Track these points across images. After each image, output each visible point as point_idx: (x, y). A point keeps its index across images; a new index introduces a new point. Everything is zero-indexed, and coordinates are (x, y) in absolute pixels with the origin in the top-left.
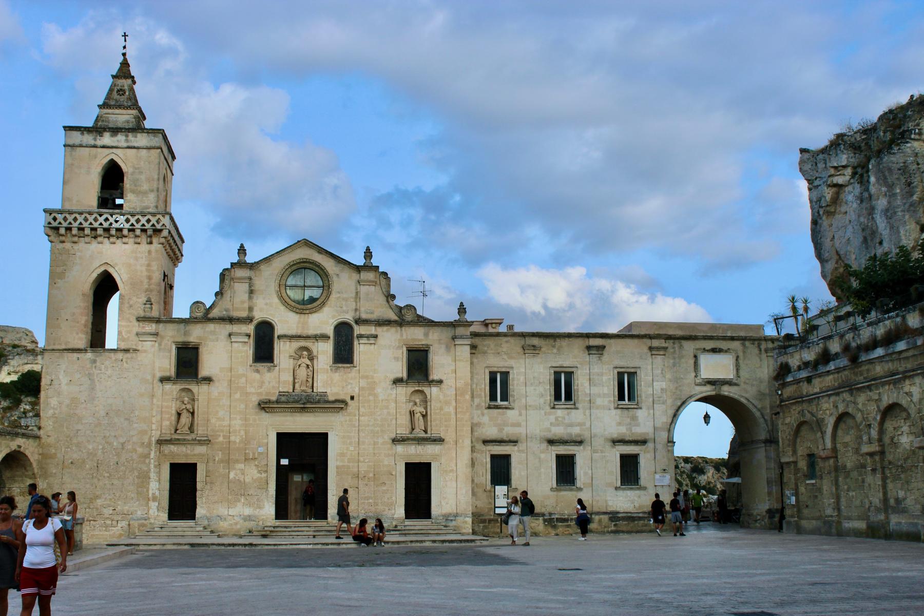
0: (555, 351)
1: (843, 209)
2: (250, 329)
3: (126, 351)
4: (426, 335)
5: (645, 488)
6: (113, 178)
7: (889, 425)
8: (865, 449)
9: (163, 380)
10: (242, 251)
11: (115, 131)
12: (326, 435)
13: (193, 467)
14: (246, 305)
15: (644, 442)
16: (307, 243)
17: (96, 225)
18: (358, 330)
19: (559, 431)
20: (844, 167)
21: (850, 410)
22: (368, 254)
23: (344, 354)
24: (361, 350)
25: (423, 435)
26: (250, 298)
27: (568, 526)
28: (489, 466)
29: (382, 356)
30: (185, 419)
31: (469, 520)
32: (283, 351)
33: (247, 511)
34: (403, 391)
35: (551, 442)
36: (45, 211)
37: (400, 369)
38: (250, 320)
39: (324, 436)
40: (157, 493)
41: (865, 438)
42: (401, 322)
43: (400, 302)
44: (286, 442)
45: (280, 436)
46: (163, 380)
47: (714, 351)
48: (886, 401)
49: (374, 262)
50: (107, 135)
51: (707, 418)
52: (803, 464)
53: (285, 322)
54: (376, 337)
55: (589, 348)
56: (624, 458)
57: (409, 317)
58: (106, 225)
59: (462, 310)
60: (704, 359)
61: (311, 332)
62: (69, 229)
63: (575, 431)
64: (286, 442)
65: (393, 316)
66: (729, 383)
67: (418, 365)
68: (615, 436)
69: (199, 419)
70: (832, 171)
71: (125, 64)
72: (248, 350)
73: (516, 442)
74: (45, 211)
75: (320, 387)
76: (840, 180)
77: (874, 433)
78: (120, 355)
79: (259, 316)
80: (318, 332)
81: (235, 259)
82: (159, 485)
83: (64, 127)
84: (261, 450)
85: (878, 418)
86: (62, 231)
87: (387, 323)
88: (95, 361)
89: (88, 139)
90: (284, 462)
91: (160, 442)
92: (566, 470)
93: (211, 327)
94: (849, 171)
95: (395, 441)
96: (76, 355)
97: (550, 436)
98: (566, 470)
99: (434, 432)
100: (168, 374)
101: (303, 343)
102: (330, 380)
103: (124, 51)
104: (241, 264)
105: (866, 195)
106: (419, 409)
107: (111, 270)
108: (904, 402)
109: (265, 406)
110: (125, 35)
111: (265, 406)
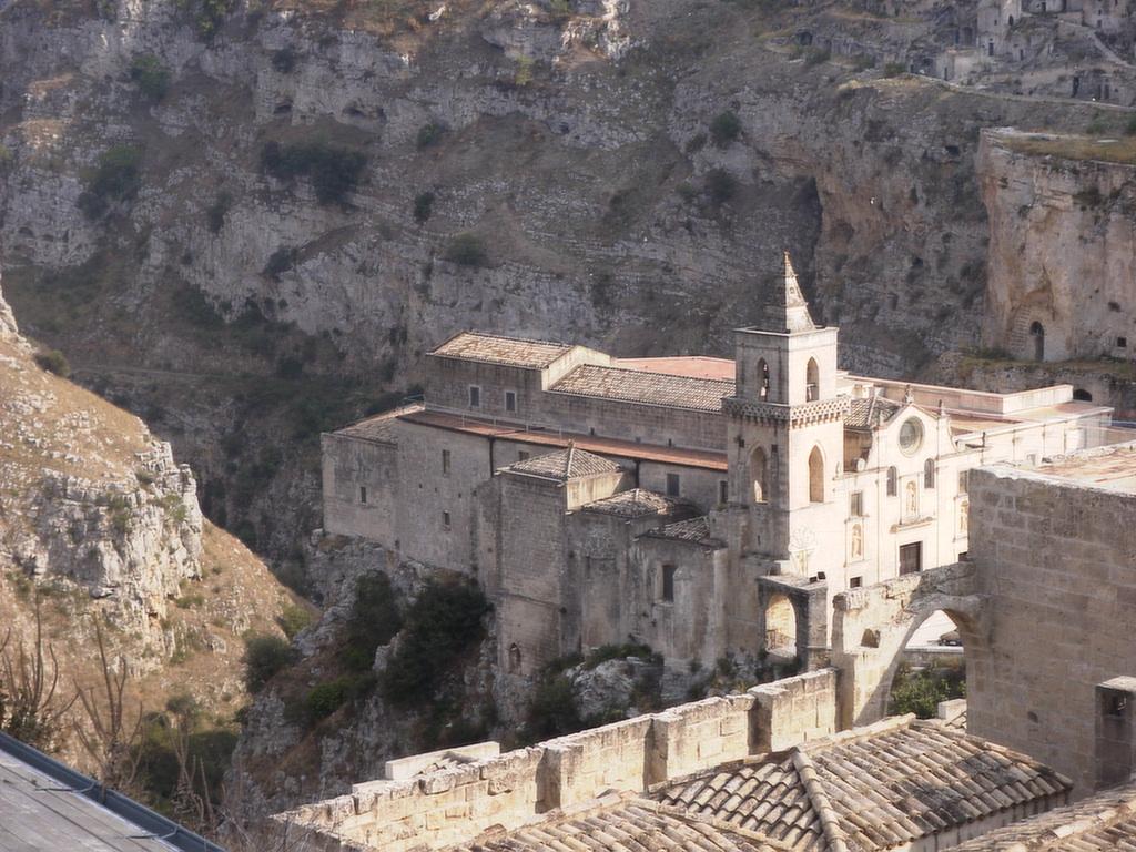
1: (1055, 229)
2: (883, 477)
20: (1064, 193)
29: (948, 480)
32: (901, 485)
39: (918, 546)
42: (957, 454)
70: (1050, 194)
72: (884, 487)
76: (1058, 204)
107: (819, 446)
109: (893, 529)
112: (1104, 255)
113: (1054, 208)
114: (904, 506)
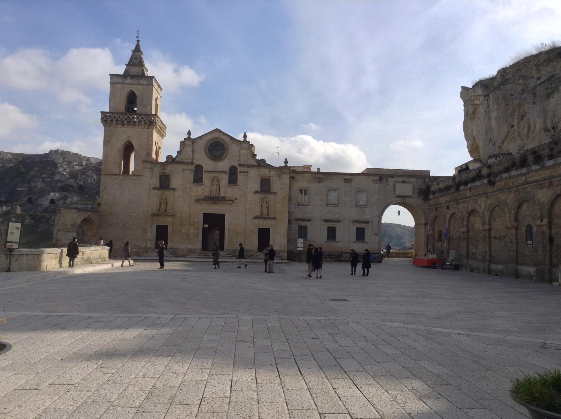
0: (329, 181)
2: (193, 167)
3: (138, 176)
4: (270, 172)
5: (367, 243)
6: (132, 99)
7: (472, 219)
8: (461, 230)
9: (154, 189)
10: (189, 133)
11: (133, 77)
12: (224, 215)
13: (166, 227)
14: (191, 157)
15: (368, 222)
16: (217, 130)
17: (124, 119)
18: (240, 169)
19: (329, 216)
20: (479, 96)
21: (456, 212)
22: (245, 136)
23: (233, 180)
24: (240, 178)
25: (267, 216)
26: (193, 154)
27: (332, 258)
28: (297, 230)
29: (250, 182)
30: (163, 206)
31: (286, 254)
32: (206, 178)
33: (190, 247)
34: (258, 196)
35: (326, 221)
36: (101, 112)
37: (257, 187)
38: (192, 163)
39: (224, 215)
40: (150, 237)
41: (461, 224)
43: (259, 157)
44: (207, 217)
45: (205, 215)
46: (154, 189)
47: (403, 182)
48: (470, 209)
49: (248, 139)
50: (129, 78)
51: (399, 212)
52: (436, 235)
53: (208, 164)
54: (247, 172)
55: (345, 180)
56: (358, 229)
57: (262, 164)
58: (128, 120)
59: (286, 162)
60: (398, 186)
61: (219, 170)
62: (112, 121)
63: (337, 216)
64: (207, 217)
65: (255, 164)
66: (410, 197)
67: (265, 186)
68: (355, 219)
69: (169, 206)
71: (138, 46)
72: (190, 176)
73: (310, 220)
74: (101, 112)
75: (222, 194)
76: (477, 102)
77: (465, 223)
78: (135, 178)
79: (196, 162)
80: (222, 170)
81: (186, 137)
82: (151, 234)
83: (110, 75)
84: (196, 220)
85: (467, 215)
86: (109, 122)
87: (253, 166)
88: (124, 180)
89: (120, 80)
90: (206, 226)
91: (153, 215)
92: (332, 233)
93: (175, 166)
94: (482, 98)
95: (256, 218)
96: (115, 177)
97: (325, 218)
98: (332, 233)
99: (271, 215)
100: (156, 186)
101: (215, 175)
102: (226, 191)
103: (137, 39)
104: (189, 138)
105: (488, 109)
106: (265, 205)
107: (131, 140)
108: (478, 208)
109: (198, 201)
110: (138, 32)
111: (198, 201)
112: (489, 118)
113: (478, 105)
114: (208, 189)
